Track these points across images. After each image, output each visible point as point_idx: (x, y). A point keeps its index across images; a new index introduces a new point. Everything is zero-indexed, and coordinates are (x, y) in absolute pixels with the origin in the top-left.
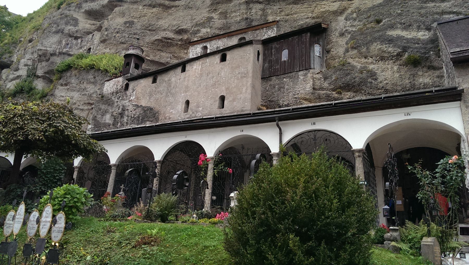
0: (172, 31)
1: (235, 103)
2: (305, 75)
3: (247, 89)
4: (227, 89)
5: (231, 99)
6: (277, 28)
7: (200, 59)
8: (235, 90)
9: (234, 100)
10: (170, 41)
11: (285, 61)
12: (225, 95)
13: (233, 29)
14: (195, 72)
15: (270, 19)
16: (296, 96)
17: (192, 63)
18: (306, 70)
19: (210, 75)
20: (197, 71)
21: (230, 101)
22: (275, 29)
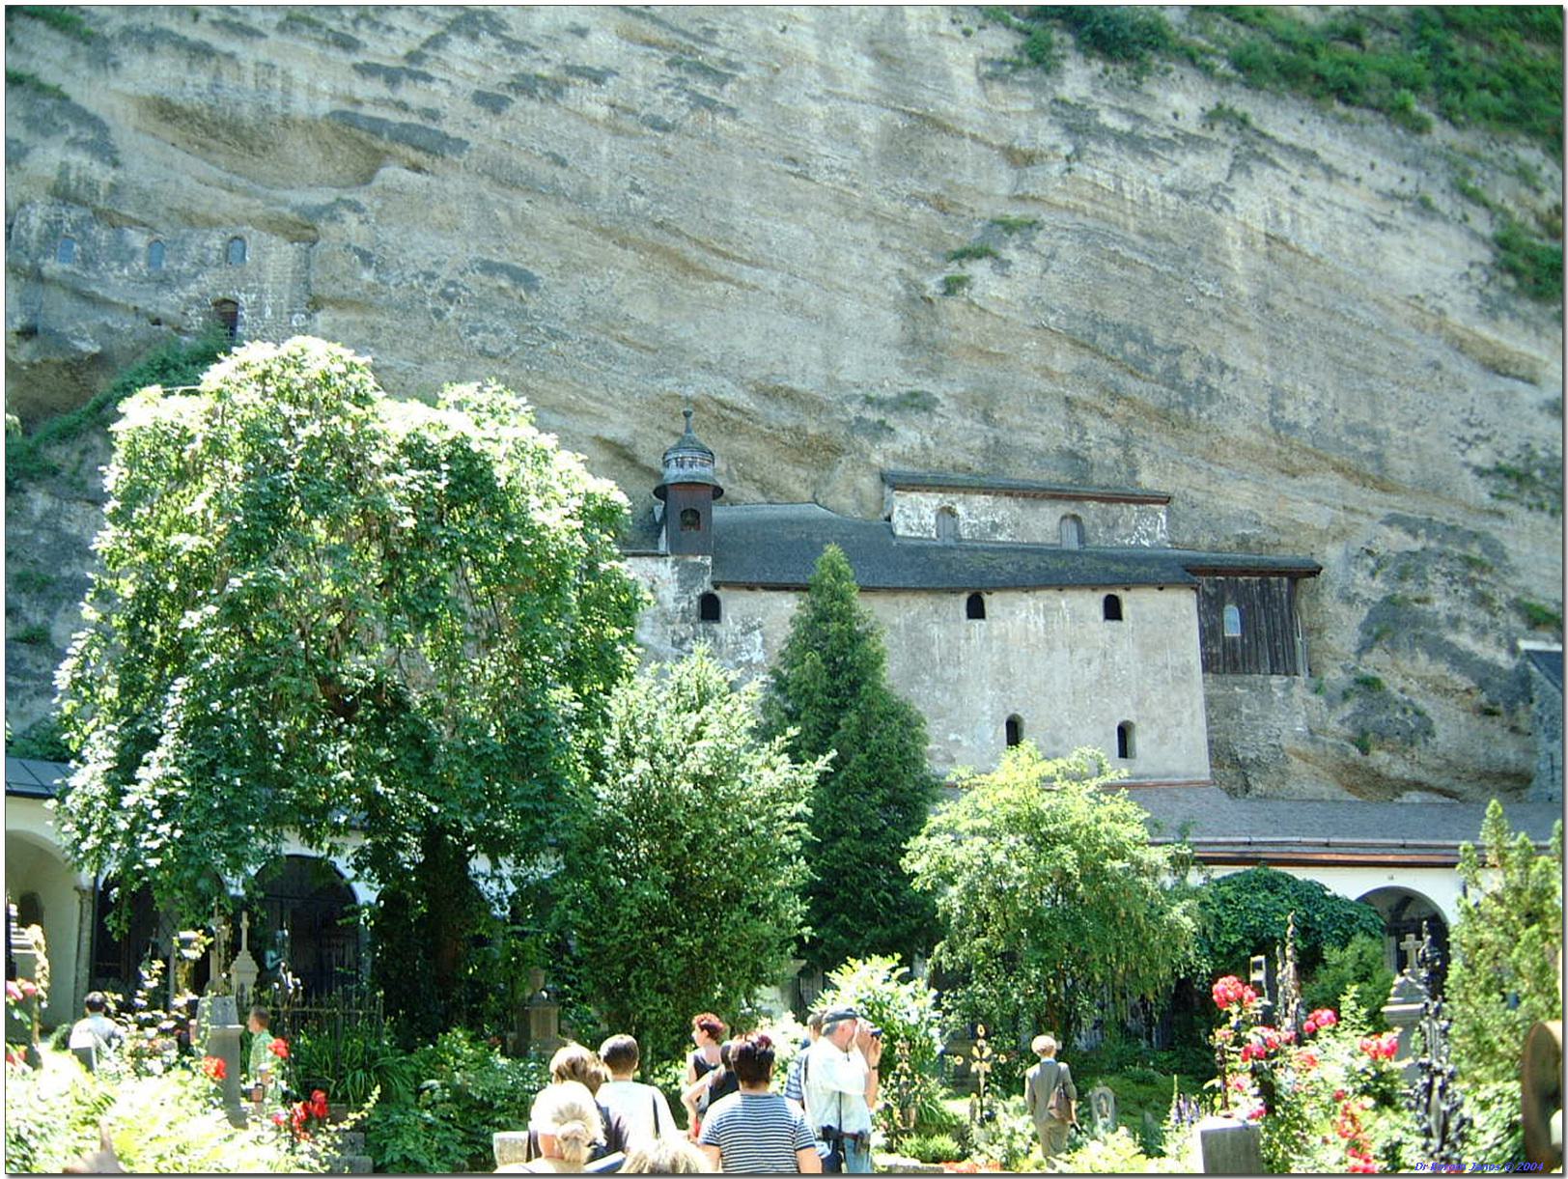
0: (741, 382)
1: (1165, 748)
2: (1287, 688)
3: (1193, 715)
4: (1139, 703)
5: (1153, 734)
6: (1168, 515)
7: (1038, 593)
8: (1160, 711)
9: (1162, 740)
10: (734, 416)
11: (1234, 639)
12: (1132, 719)
13: (1024, 472)
14: (1027, 630)
15: (1147, 480)
16: (1273, 741)
17: (1010, 596)
18: (1287, 674)
19: (1081, 653)
20: (1031, 626)
21: (1152, 741)
22: (1164, 518)
